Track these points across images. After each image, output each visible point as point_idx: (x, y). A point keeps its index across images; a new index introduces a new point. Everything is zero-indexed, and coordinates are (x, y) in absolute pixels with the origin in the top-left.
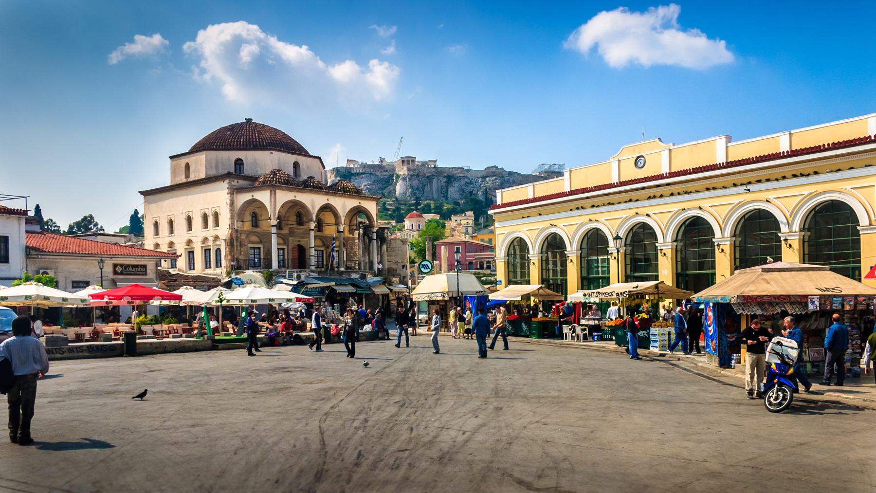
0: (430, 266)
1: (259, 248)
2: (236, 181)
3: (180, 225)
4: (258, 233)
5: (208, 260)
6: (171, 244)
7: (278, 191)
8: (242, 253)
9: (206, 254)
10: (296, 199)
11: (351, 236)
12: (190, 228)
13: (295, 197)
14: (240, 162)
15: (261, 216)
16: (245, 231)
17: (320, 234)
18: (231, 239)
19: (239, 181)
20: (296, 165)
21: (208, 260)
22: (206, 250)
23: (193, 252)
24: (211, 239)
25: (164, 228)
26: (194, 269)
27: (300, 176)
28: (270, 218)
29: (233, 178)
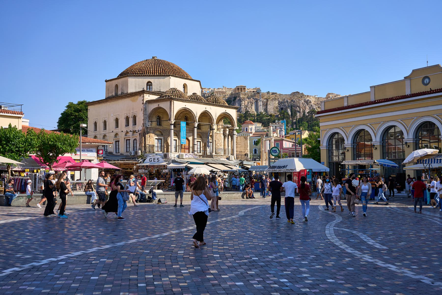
0: (278, 152)
1: (161, 139)
2: (148, 95)
3: (111, 124)
4: (160, 129)
7: (175, 101)
8: (151, 142)
9: (127, 143)
11: (219, 132)
12: (117, 126)
14: (150, 84)
15: (163, 118)
16: (153, 128)
17: (199, 131)
18: (144, 133)
19: (150, 95)
20: (185, 86)
22: (127, 140)
23: (119, 141)
25: (100, 125)
26: (119, 153)
27: (187, 93)
28: (170, 119)
29: (146, 93)
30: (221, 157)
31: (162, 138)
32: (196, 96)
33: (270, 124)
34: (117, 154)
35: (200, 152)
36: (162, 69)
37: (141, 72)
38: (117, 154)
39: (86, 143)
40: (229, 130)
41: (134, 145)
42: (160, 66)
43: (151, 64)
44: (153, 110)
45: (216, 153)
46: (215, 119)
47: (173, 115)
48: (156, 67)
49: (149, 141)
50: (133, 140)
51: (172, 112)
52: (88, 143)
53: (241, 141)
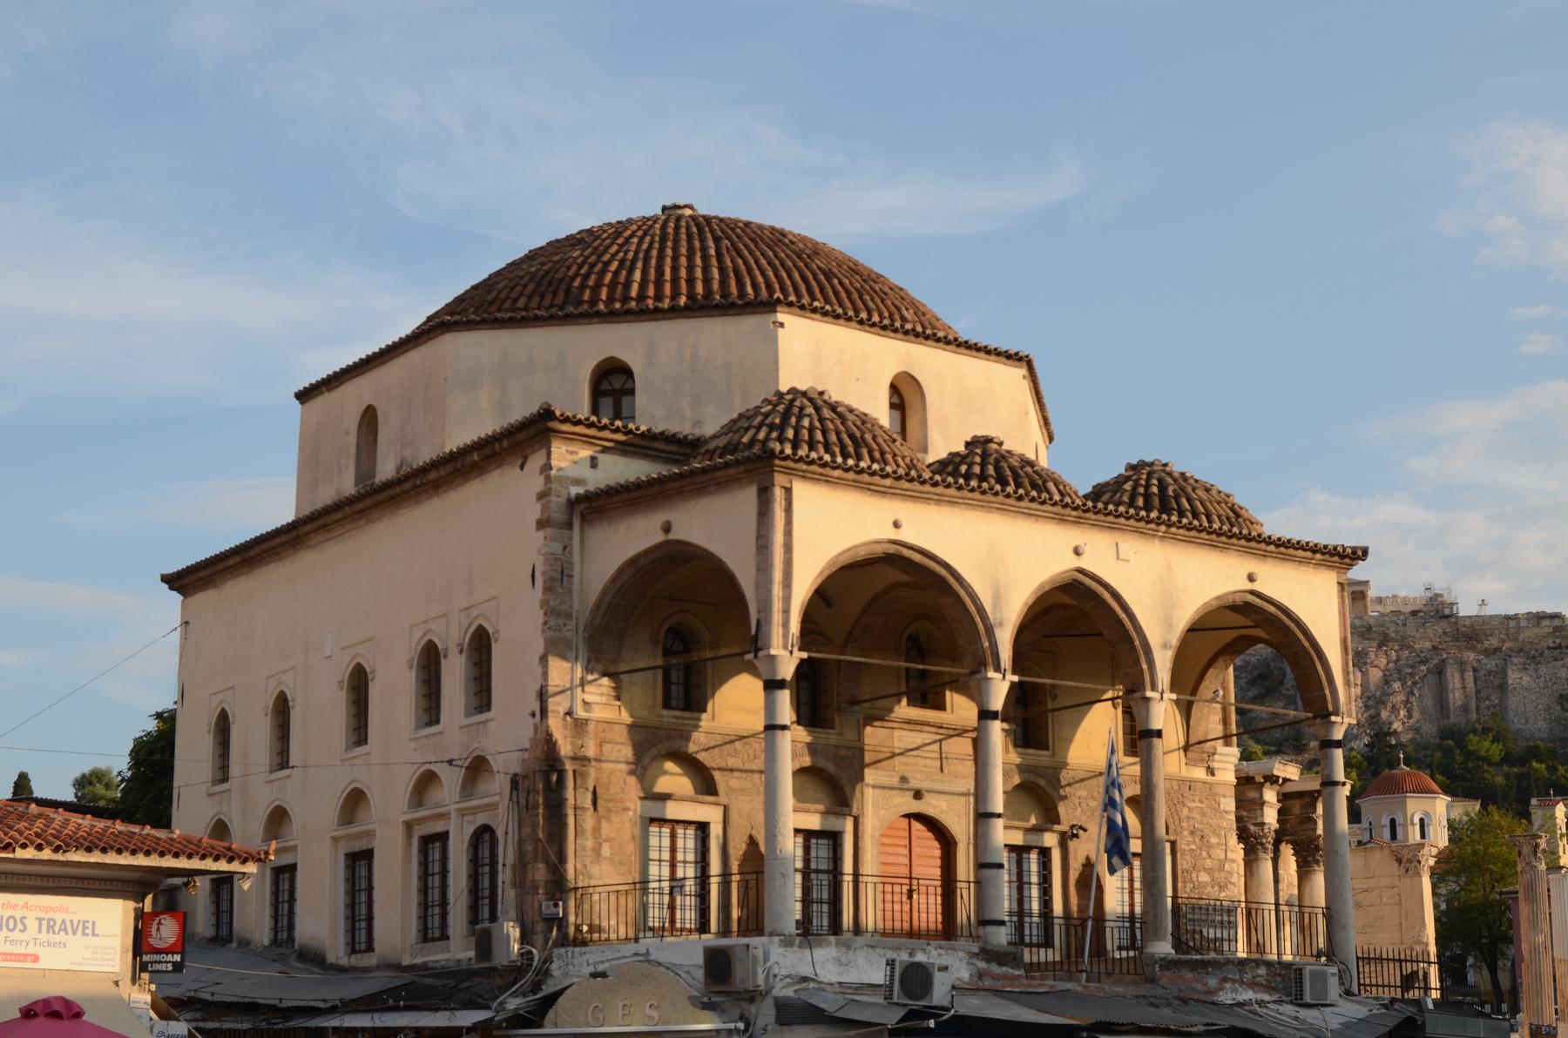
1: (702, 828)
5: (435, 896)
6: (278, 818)
7: (801, 490)
8: (606, 850)
10: (904, 535)
11: (1199, 773)
13: (896, 525)
20: (904, 394)
21: (435, 896)
24: (451, 779)
25: (251, 735)
26: (370, 948)
28: (756, 638)
30: (1225, 980)
31: (708, 813)
32: (992, 460)
33: (1534, 801)
34: (356, 961)
35: (1047, 943)
36: (722, 270)
37: (555, 294)
38: (356, 961)
39: (20, 854)
40: (1284, 798)
41: (474, 878)
42: (704, 249)
43: (635, 240)
44: (621, 571)
45: (1178, 944)
46: (1165, 646)
47: (787, 599)
48: (675, 258)
49: (589, 844)
50: (467, 838)
51: (778, 575)
52: (30, 853)
53: (1373, 883)
